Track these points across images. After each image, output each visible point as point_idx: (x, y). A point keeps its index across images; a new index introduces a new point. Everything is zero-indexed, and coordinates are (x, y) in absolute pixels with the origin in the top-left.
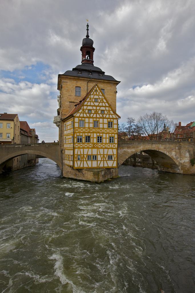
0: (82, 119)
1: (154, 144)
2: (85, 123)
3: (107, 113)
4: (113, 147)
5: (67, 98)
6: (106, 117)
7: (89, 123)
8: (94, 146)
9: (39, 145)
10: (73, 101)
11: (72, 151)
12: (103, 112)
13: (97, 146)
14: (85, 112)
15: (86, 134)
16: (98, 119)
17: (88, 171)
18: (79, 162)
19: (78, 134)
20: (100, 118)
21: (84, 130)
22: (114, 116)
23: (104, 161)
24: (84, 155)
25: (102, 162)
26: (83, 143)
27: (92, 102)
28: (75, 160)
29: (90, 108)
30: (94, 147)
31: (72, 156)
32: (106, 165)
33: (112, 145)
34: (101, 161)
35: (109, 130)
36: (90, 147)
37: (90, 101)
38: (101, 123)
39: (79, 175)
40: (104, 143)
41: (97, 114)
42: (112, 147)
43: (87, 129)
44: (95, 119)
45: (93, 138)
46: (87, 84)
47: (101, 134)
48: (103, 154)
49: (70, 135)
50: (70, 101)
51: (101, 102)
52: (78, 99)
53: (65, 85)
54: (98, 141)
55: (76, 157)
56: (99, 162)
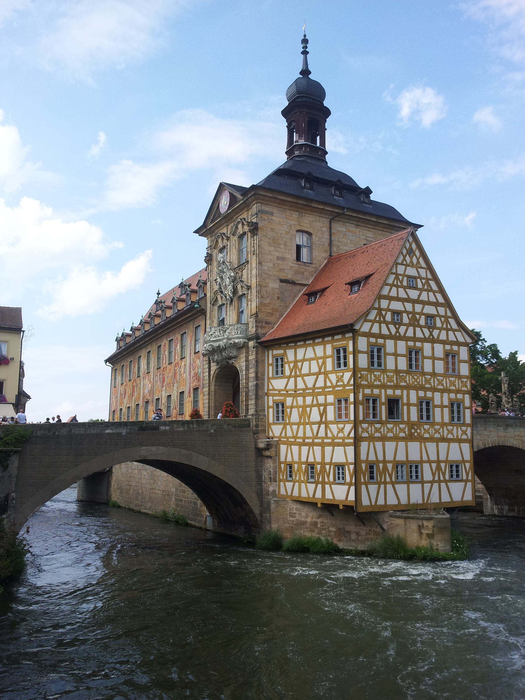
0: (377, 341)
1: (512, 426)
2: (386, 354)
3: (442, 323)
4: (462, 435)
5: (271, 265)
6: (439, 335)
7: (396, 355)
8: (413, 431)
9: (186, 428)
10: (289, 276)
11: (351, 450)
12: (431, 320)
13: (419, 431)
14: (384, 317)
15: (390, 392)
16: (418, 344)
17: (406, 518)
18: (373, 488)
19: (367, 391)
20: (424, 340)
21: (384, 379)
22: (461, 337)
23: (439, 482)
24: (385, 462)
25: (436, 485)
26: (380, 422)
27: (402, 287)
28: (363, 481)
29: (396, 306)
30: (410, 438)
31: (340, 467)
32: (446, 498)
33: (457, 429)
34: (432, 482)
35: (448, 381)
36: (402, 435)
37: (395, 283)
38: (427, 358)
39: (358, 534)
40: (438, 424)
41: (417, 328)
42: (457, 436)
43: (393, 377)
44: (411, 344)
45: (409, 405)
46: (328, 225)
47: (429, 394)
48: (435, 458)
49: (326, 394)
50: (283, 276)
51: (425, 290)
52: (303, 273)
53: (266, 223)
54: (422, 418)
55: (364, 469)
56: (427, 486)
